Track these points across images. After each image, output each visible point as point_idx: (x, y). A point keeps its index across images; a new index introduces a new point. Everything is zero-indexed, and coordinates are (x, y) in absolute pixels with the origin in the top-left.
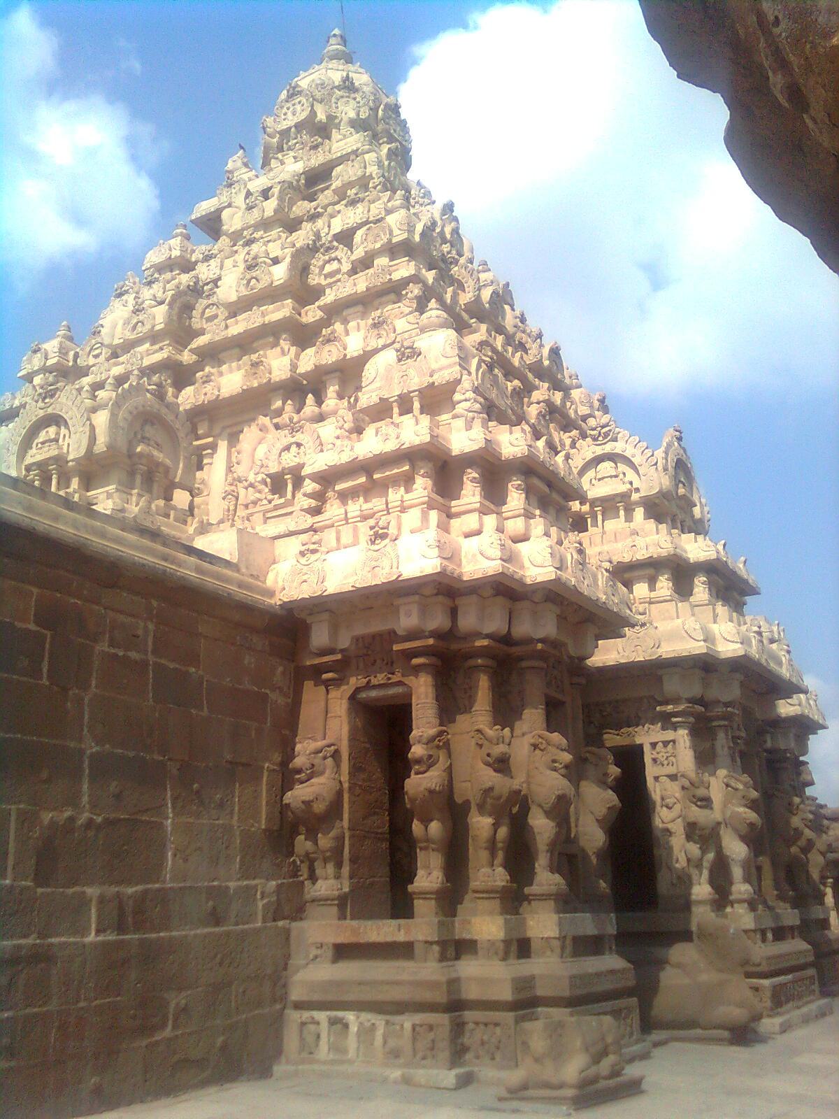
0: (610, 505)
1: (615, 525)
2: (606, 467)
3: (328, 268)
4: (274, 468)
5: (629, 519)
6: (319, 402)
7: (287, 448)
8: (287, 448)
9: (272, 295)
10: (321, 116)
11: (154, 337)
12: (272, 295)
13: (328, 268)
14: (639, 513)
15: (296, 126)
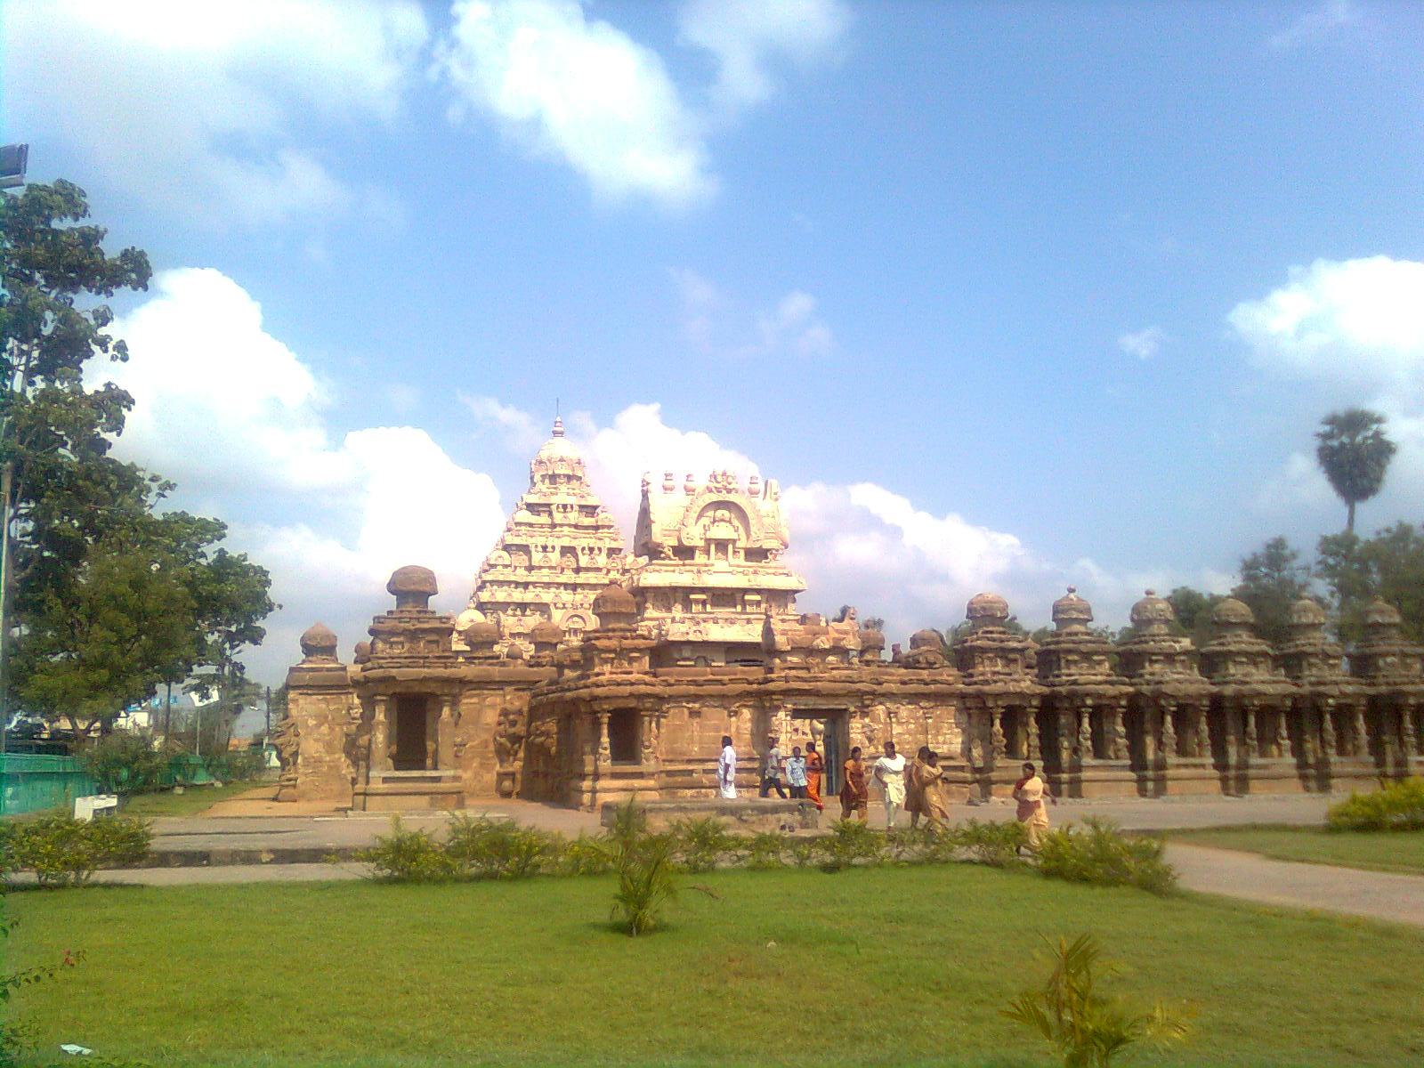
3: (613, 565)
10: (571, 474)
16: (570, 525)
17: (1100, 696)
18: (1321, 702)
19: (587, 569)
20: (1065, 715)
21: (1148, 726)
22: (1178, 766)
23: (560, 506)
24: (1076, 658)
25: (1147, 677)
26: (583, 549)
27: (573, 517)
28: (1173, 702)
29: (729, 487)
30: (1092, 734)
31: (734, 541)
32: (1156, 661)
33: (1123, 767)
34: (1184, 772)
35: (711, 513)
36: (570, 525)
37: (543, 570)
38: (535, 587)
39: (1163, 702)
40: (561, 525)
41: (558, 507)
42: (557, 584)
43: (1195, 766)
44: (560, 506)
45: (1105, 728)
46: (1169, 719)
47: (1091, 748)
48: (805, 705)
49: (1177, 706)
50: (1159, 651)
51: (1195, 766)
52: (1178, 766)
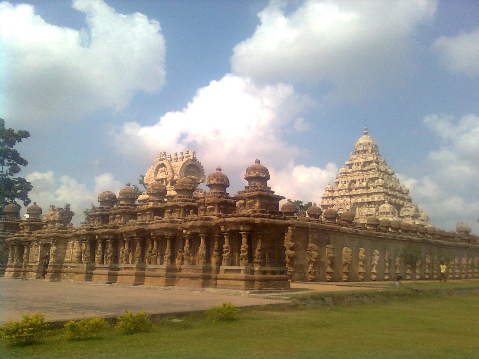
0: (407, 216)
1: (408, 218)
2: (407, 211)
3: (371, 185)
4: (367, 214)
5: (409, 218)
6: (371, 205)
7: (368, 212)
8: (368, 212)
9: (363, 188)
10: (365, 149)
11: (345, 189)
12: (363, 188)
13: (371, 185)
14: (411, 217)
15: (361, 150)
16: (359, 171)
19: (360, 188)
23: (357, 163)
26: (359, 180)
27: (360, 167)
29: (162, 158)
31: (166, 179)
35: (160, 169)
36: (359, 171)
37: (343, 191)
38: (339, 198)
40: (356, 171)
41: (355, 164)
42: (347, 195)
44: (357, 163)
48: (44, 242)
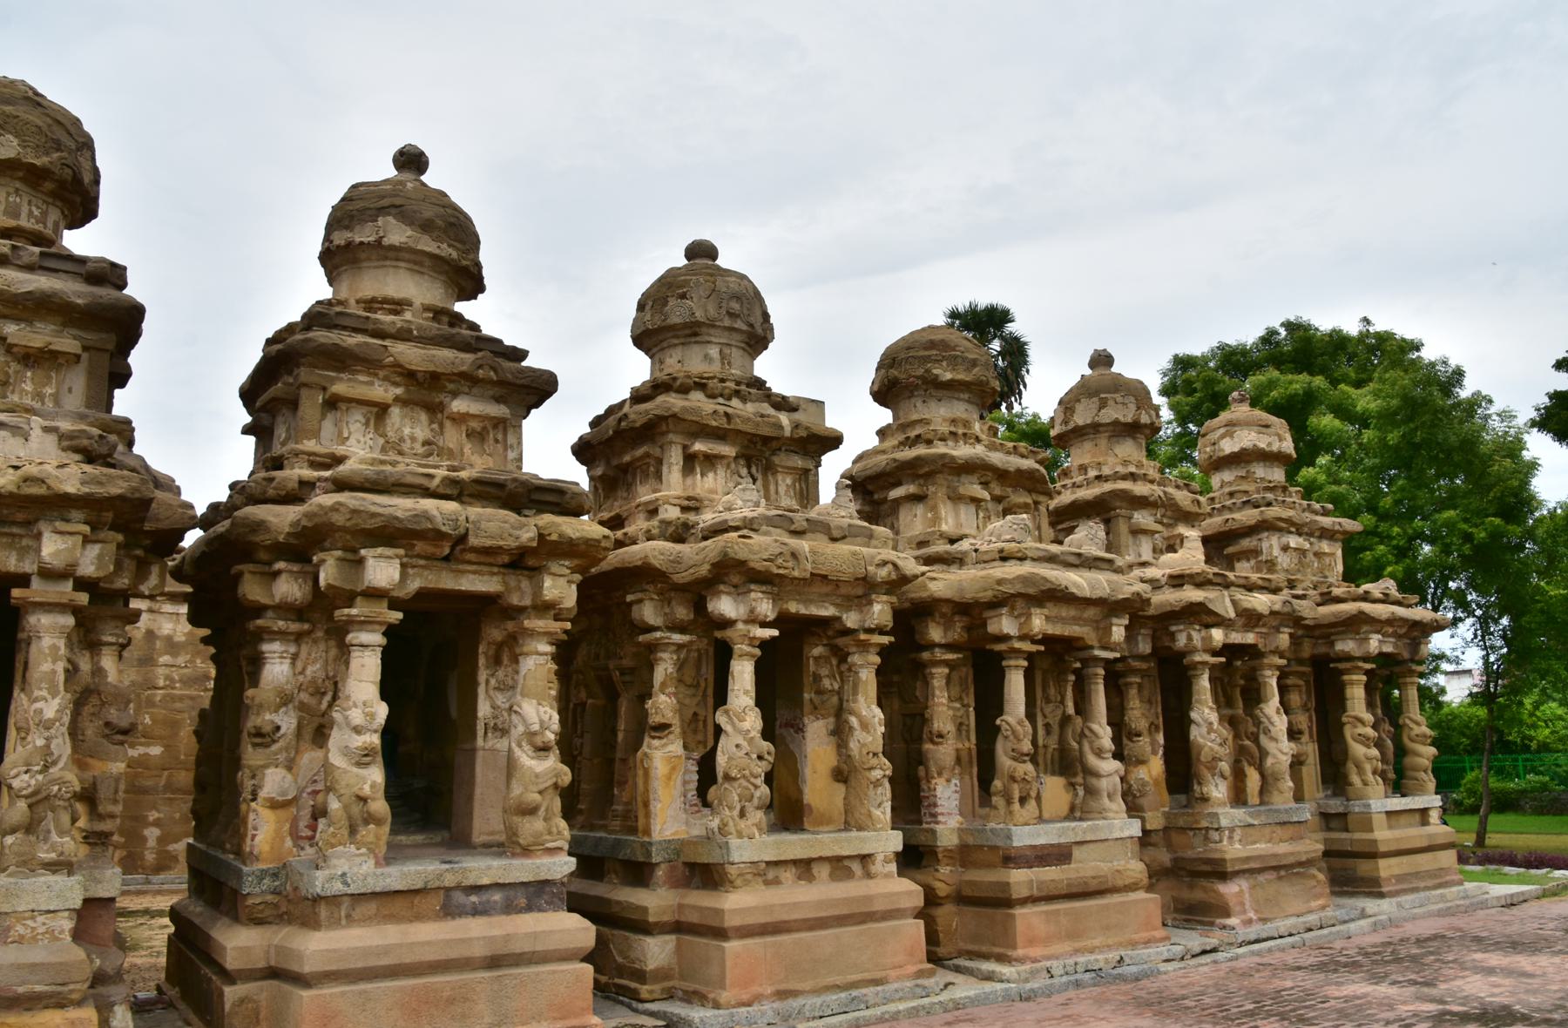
17: (455, 547)
18: (1186, 637)
20: (282, 635)
21: (663, 705)
22: (769, 871)
24: (381, 391)
25: (672, 513)
28: (766, 609)
30: (388, 732)
32: (710, 461)
33: (536, 894)
34: (796, 896)
39: (725, 606)
43: (839, 866)
45: (484, 709)
46: (743, 674)
47: (380, 806)
49: (782, 621)
50: (723, 422)
51: (839, 866)
52: (769, 871)
